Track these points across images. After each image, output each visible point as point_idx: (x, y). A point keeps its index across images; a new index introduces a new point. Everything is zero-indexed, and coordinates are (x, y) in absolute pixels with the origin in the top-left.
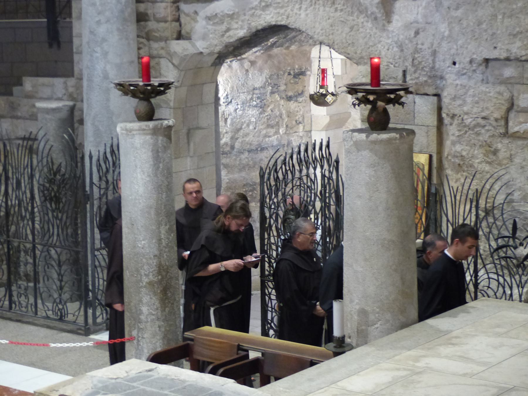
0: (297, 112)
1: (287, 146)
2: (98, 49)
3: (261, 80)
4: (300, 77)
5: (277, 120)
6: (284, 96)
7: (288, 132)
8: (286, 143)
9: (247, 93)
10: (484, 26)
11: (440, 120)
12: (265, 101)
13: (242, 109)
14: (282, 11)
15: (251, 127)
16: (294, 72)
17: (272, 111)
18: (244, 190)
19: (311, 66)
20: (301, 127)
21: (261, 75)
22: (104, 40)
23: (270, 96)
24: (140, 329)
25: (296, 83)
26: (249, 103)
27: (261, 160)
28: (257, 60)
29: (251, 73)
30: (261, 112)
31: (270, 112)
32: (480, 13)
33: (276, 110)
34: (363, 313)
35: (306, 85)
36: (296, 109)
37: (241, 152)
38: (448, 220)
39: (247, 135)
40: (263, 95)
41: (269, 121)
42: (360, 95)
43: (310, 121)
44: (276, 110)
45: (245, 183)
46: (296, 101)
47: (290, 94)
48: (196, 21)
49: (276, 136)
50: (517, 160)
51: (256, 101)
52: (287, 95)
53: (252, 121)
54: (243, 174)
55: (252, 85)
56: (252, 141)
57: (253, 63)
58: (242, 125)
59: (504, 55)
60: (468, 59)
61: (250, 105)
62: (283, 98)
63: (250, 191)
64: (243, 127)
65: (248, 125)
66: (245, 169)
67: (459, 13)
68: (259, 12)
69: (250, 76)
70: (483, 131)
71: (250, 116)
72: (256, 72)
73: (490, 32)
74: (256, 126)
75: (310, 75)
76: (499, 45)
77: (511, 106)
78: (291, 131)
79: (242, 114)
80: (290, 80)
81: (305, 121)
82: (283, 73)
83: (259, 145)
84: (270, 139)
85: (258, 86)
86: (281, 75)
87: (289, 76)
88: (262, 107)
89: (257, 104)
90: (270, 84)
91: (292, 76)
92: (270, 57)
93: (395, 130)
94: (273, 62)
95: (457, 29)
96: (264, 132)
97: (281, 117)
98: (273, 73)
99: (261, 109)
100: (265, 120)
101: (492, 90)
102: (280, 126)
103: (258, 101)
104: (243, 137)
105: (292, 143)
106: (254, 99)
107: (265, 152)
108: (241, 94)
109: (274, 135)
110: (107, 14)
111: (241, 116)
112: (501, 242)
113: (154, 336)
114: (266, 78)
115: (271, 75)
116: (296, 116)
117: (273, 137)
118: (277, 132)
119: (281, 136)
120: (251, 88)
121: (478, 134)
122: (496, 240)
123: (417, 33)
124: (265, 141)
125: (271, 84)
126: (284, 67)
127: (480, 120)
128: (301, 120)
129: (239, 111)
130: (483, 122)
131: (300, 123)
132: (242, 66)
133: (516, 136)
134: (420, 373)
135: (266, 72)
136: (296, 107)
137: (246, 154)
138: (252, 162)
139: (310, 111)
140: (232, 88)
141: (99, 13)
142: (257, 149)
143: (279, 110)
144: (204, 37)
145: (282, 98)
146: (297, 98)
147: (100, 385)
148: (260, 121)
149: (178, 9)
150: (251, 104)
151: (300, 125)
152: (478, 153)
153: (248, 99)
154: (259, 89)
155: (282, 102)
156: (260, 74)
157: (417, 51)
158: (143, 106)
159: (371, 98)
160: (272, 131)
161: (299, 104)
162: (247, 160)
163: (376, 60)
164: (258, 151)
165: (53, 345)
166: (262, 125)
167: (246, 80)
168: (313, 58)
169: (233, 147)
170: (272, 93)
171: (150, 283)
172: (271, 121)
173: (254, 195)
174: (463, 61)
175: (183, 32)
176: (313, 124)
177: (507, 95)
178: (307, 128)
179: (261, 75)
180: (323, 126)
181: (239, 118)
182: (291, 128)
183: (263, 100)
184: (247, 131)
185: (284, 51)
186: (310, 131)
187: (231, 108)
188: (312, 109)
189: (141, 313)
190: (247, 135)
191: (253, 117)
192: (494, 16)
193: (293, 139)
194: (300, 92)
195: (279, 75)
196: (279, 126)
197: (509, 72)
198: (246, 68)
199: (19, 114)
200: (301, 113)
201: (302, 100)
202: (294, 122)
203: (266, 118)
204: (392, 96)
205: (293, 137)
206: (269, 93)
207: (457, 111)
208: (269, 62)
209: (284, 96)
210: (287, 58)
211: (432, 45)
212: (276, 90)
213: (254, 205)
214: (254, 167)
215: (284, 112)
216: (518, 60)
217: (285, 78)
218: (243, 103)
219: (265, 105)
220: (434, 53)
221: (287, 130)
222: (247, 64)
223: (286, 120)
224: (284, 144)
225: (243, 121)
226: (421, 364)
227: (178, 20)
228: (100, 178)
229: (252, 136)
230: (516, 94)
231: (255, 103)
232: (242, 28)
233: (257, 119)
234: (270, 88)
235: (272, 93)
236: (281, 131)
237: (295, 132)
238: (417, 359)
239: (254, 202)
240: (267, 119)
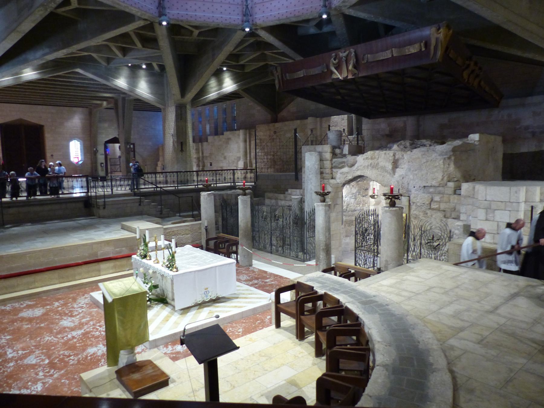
2: (309, 182)
10: (424, 176)
11: (410, 204)
14: (362, 171)
22: (311, 179)
24: (320, 262)
32: (423, 172)
34: (386, 261)
37: (349, 211)
38: (412, 234)
39: (351, 206)
42: (387, 196)
47: (364, 195)
48: (337, 174)
50: (434, 216)
54: (350, 218)
57: (353, 186)
59: (430, 185)
60: (419, 186)
65: (351, 204)
67: (416, 172)
68: (355, 172)
70: (423, 207)
73: (426, 178)
76: (429, 182)
77: (432, 200)
83: (354, 209)
88: (356, 199)
92: (358, 184)
93: (397, 207)
95: (415, 177)
96: (356, 206)
101: (426, 196)
110: (312, 172)
111: (349, 201)
112: (429, 241)
113: (324, 264)
118: (360, 206)
121: (421, 208)
122: (427, 240)
123: (403, 178)
127: (422, 204)
130: (423, 205)
132: (350, 187)
133: (433, 209)
134: (404, 280)
135: (357, 189)
137: (350, 212)
140: (347, 193)
141: (310, 172)
144: (340, 179)
147: (309, 279)
149: (332, 170)
152: (421, 214)
155: (361, 197)
157: (403, 183)
158: (322, 198)
159: (390, 197)
160: (358, 205)
163: (392, 186)
165: (295, 265)
169: (347, 210)
170: (358, 195)
171: (323, 249)
174: (417, 186)
175: (333, 177)
177: (431, 197)
187: (346, 199)
189: (320, 257)
190: (351, 206)
192: (427, 173)
197: (431, 190)
199: (287, 199)
204: (397, 197)
207: (415, 201)
211: (408, 181)
215: (362, 200)
216: (434, 186)
220: (408, 184)
222: (351, 186)
226: (404, 278)
227: (332, 174)
228: (309, 218)
230: (433, 196)
235: (358, 195)
238: (403, 276)
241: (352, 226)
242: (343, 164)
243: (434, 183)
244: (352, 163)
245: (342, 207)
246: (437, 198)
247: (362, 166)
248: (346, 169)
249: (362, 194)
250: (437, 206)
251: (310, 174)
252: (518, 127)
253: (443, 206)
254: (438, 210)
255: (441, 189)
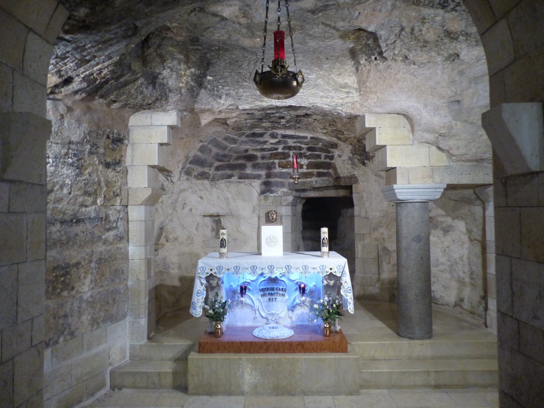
0: (115, 182)
1: (105, 219)
3: (78, 132)
4: (119, 144)
5: (95, 188)
6: (103, 161)
7: (105, 204)
8: (103, 215)
9: (61, 144)
12: (82, 161)
13: (54, 164)
15: (65, 191)
16: (113, 137)
17: (90, 175)
18: (54, 274)
19: (128, 136)
20: (118, 199)
21: (79, 128)
23: (89, 156)
25: (113, 150)
26: (64, 158)
27: (77, 235)
28: (74, 107)
29: (67, 121)
30: (77, 174)
31: (88, 176)
33: (95, 175)
35: (123, 154)
36: (114, 179)
39: (59, 200)
40: (81, 153)
41: (87, 187)
43: (127, 195)
44: (95, 175)
45: (56, 265)
46: (115, 170)
47: (108, 160)
49: (94, 207)
51: (71, 158)
52: (105, 161)
53: (66, 182)
55: (68, 137)
56: (66, 209)
57: (70, 109)
58: (54, 186)
61: (65, 162)
62: (102, 163)
63: (61, 276)
64: (55, 189)
65: (61, 188)
66: (56, 247)
69: (66, 124)
71: (65, 176)
72: (73, 121)
74: (71, 191)
75: (127, 145)
78: (109, 204)
79: (54, 172)
80: (108, 145)
81: (123, 194)
82: (102, 133)
83: (75, 215)
84: (88, 209)
85: (75, 140)
86: (100, 135)
87: (107, 140)
88: (80, 168)
89: (73, 162)
90: (88, 142)
91: (111, 141)
92: (89, 109)
94: (92, 117)
96: (81, 199)
97: (99, 185)
98: (92, 130)
99: (77, 170)
100: (82, 184)
102: (98, 195)
103: (75, 159)
104: (54, 203)
105: (109, 217)
106: (70, 156)
107: (82, 225)
108: (53, 144)
109: (91, 205)
114: (84, 132)
115: (90, 132)
116: (114, 187)
117: (90, 208)
118: (94, 203)
119: (99, 207)
120: (67, 141)
124: (82, 211)
125: (89, 142)
126: (104, 127)
128: (118, 191)
129: (50, 166)
131: (117, 195)
135: (85, 126)
136: (113, 177)
137: (58, 226)
138: (65, 237)
139: (127, 184)
142: (72, 221)
143: (98, 176)
145: (101, 162)
146: (115, 167)
148: (76, 184)
150: (66, 160)
151: (118, 197)
153: (63, 153)
154: (77, 144)
155: (100, 167)
156: (77, 125)
160: (90, 200)
161: (117, 174)
162: (58, 234)
164: (73, 223)
166: (79, 190)
167: (60, 128)
168: (131, 126)
170: (91, 153)
172: (89, 188)
173: (67, 281)
176: (130, 198)
178: (125, 204)
179: (79, 128)
180: (143, 200)
181: (50, 176)
182: (109, 200)
183: (80, 159)
184: (61, 195)
185: (105, 108)
186: (127, 206)
188: (128, 182)
190: (59, 200)
191: (69, 178)
193: (110, 212)
194: (117, 161)
195: (99, 134)
196: (96, 195)
198: (62, 113)
200: (119, 184)
201: (120, 170)
202: (112, 194)
203: (83, 182)
205: (110, 210)
206: (87, 152)
208: (88, 115)
209: (103, 161)
210: (106, 117)
212: (95, 151)
213: (67, 295)
214: (68, 243)
215: (102, 179)
217: (104, 141)
218: (56, 157)
219: (82, 166)
221: (104, 202)
222: (62, 108)
223: (105, 189)
224: (102, 218)
225: (55, 180)
229: (66, 203)
231: (70, 160)
233: (73, 181)
234: (89, 147)
236: (98, 201)
237: (112, 206)
239: (67, 289)
240: (85, 184)
241: (65, 293)
245: (46, 179)
249: (104, 155)
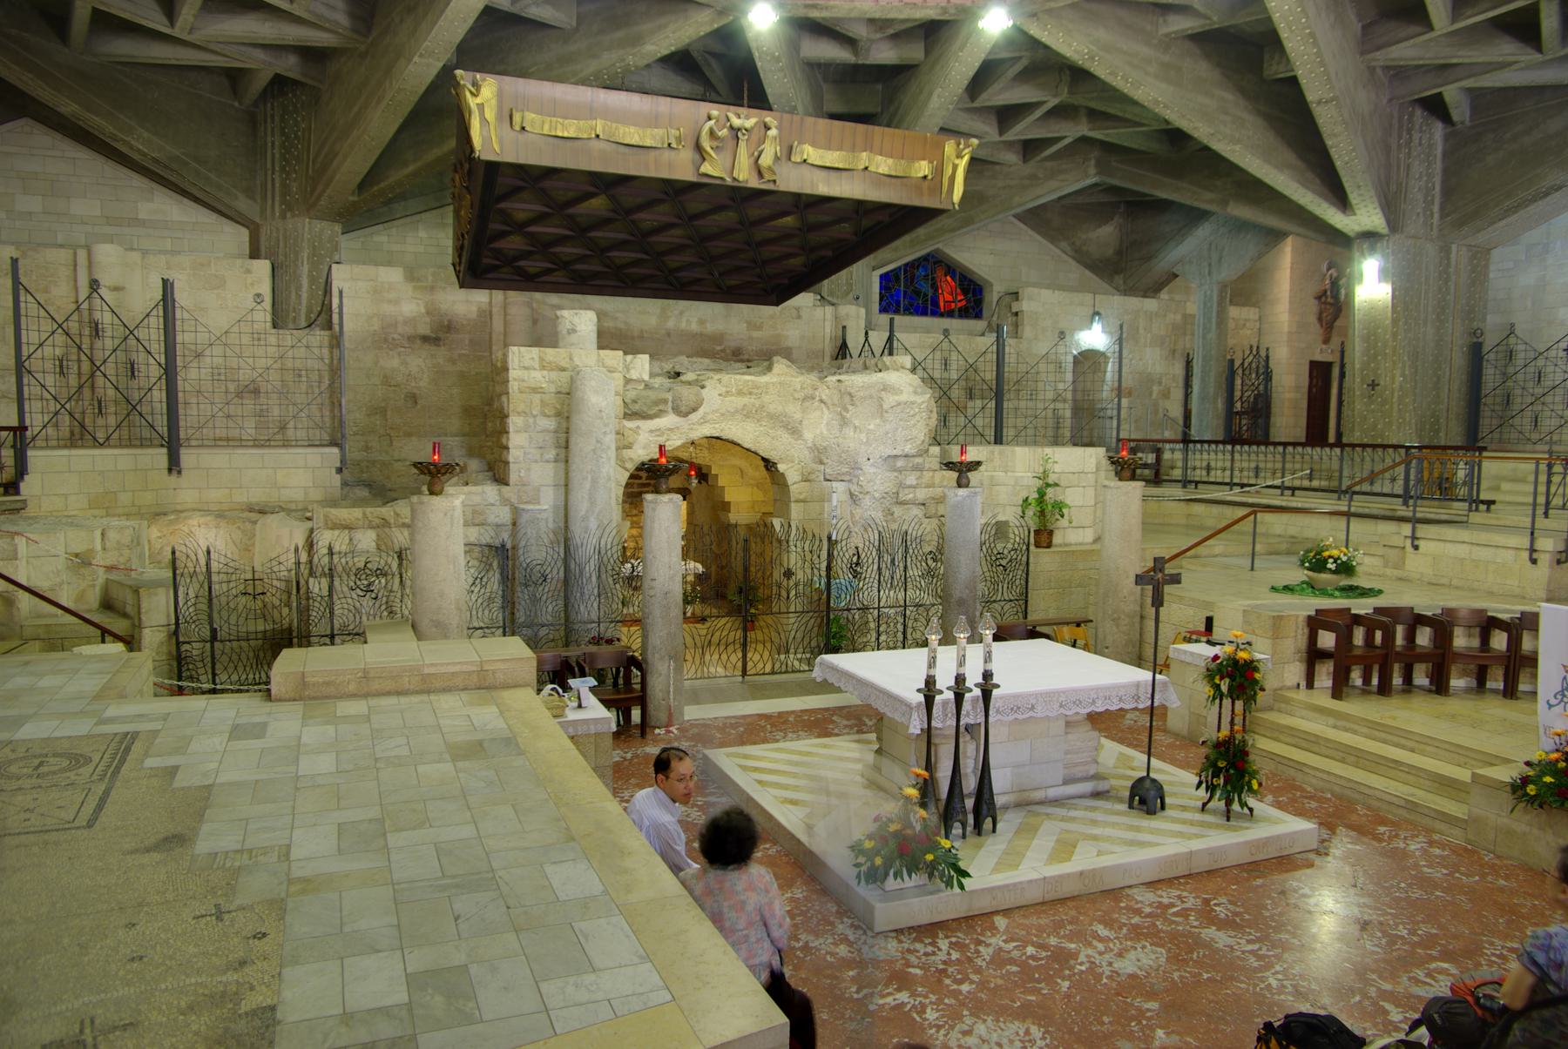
48: (639, 434)
141: (606, 425)
197: (900, 463)
232: (680, 438)
242: (661, 407)
243: (908, 449)
244: (693, 404)
246: (911, 479)
247: (716, 411)
248: (669, 420)
250: (911, 496)
251: (605, 433)
252: (719, 348)
253: (922, 494)
254: (913, 503)
255: (919, 460)
